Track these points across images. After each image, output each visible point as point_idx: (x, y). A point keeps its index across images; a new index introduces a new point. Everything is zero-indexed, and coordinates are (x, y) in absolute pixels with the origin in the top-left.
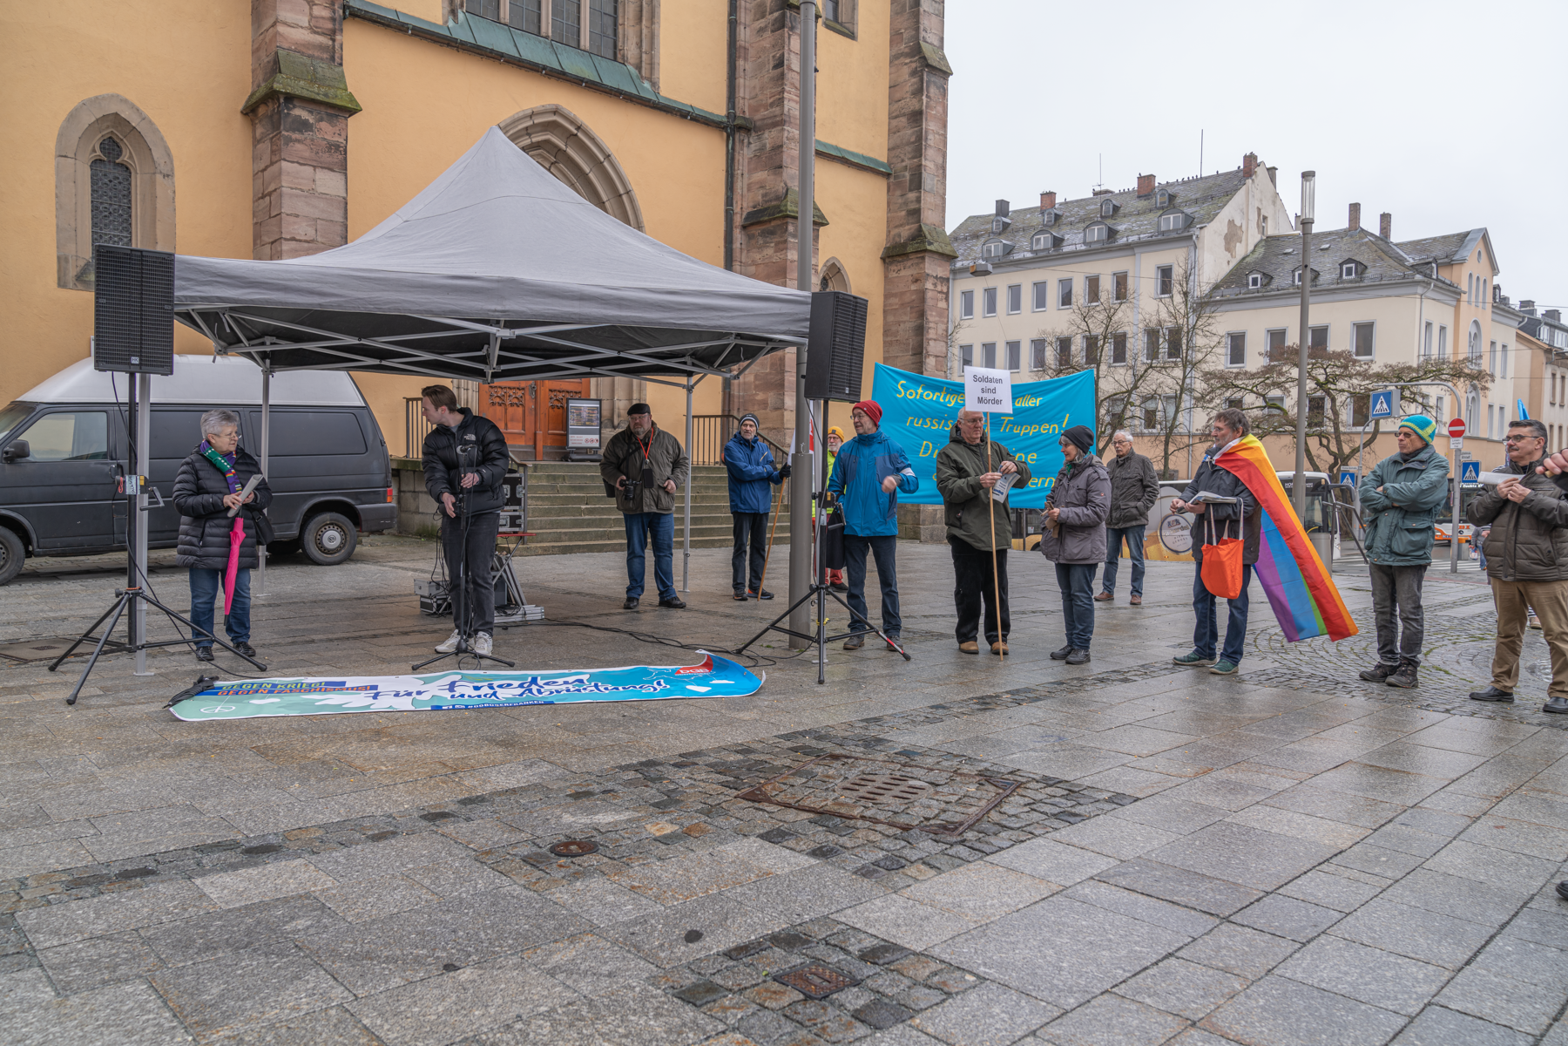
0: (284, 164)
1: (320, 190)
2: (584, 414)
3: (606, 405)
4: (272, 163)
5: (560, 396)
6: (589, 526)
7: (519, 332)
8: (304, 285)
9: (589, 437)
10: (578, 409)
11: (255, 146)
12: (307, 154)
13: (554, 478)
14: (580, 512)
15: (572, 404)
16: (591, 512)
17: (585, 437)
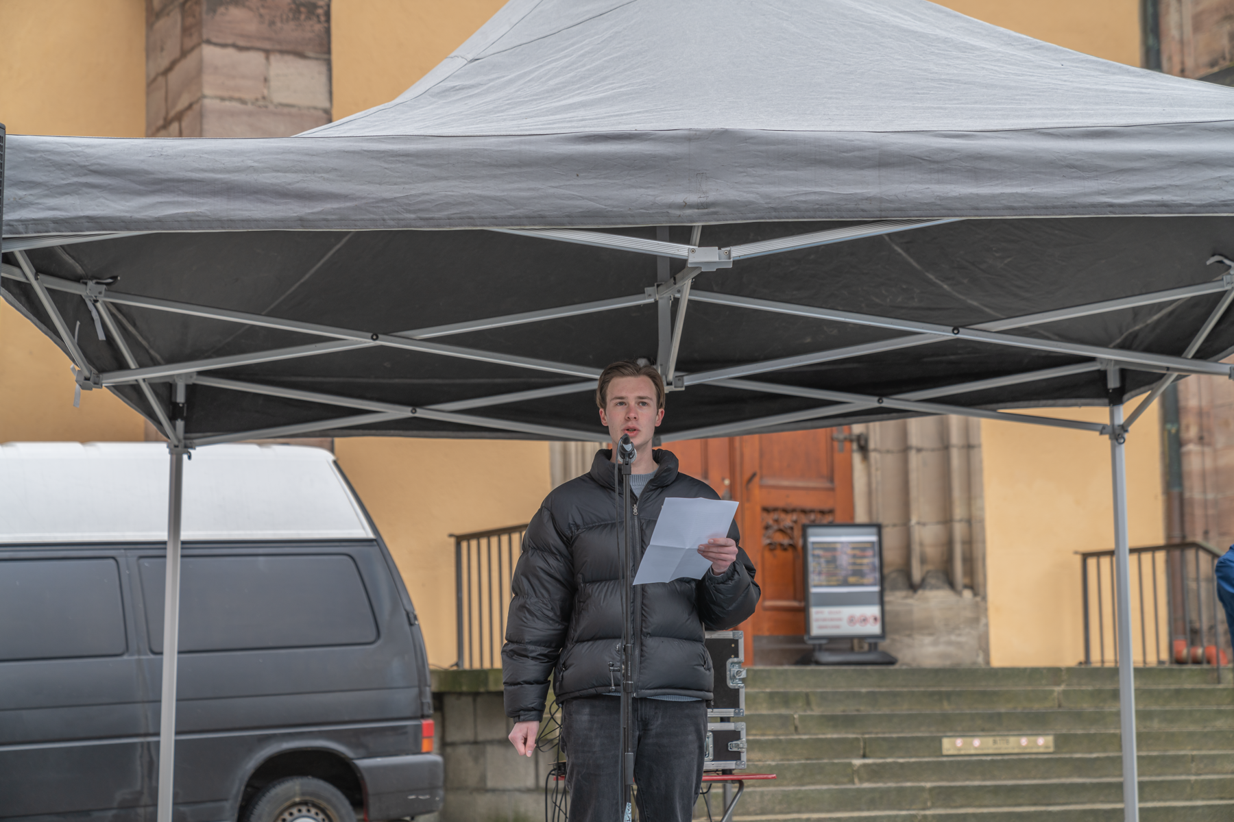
0: (208, 51)
1: (279, 97)
2: (844, 560)
3: (892, 538)
4: (184, 54)
5: (787, 520)
6: (872, 804)
7: (740, 251)
8: (268, 179)
10: (830, 548)
11: (150, 25)
12: (252, 27)
13: (787, 699)
14: (851, 773)
16: (875, 773)
17: (847, 611)
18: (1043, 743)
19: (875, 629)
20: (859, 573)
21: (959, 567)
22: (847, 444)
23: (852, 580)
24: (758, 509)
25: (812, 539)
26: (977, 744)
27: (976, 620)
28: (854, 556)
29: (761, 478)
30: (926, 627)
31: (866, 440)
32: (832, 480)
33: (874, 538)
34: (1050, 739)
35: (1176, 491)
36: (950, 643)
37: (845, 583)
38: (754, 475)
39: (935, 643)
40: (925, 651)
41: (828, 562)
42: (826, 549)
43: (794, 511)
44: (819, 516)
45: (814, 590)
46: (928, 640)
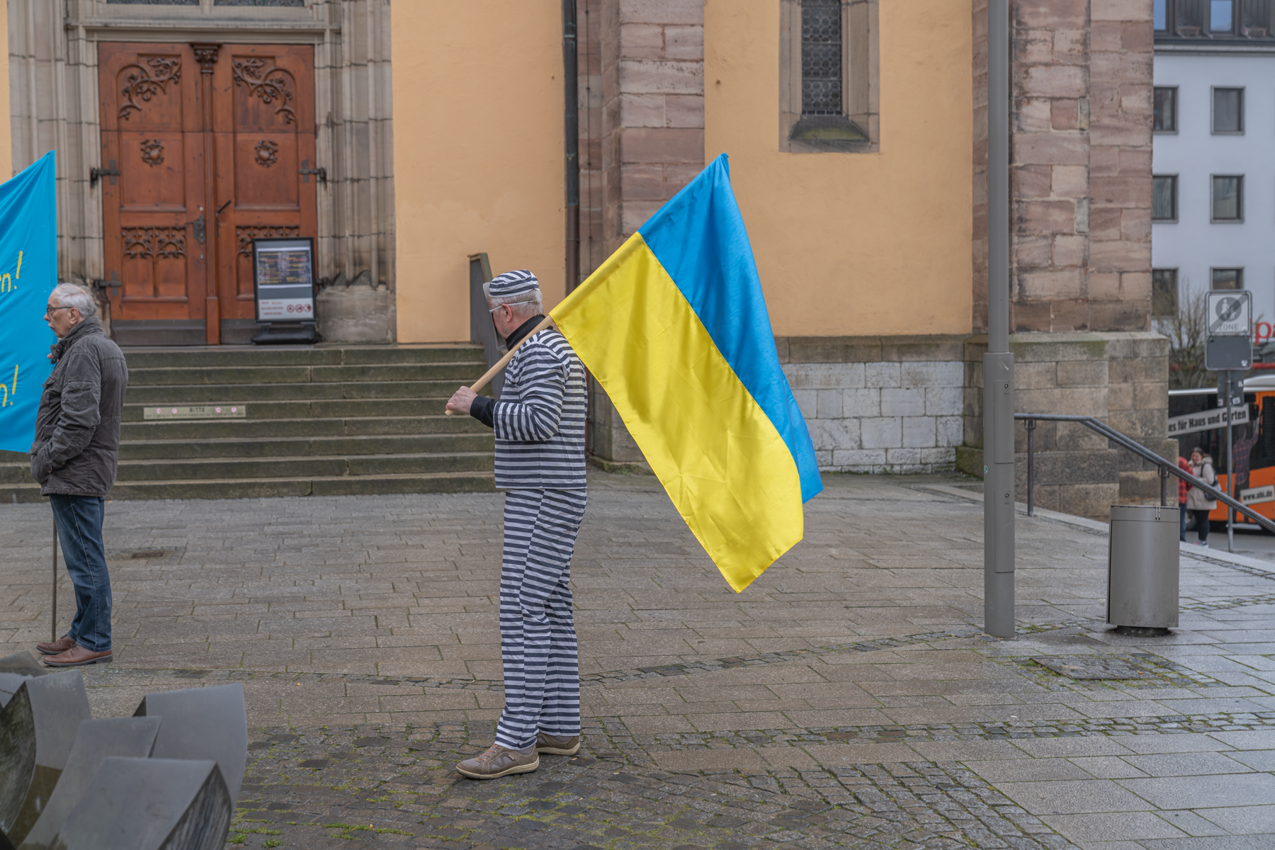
2: (283, 265)
3: (324, 245)
9: (295, 302)
10: (273, 256)
15: (261, 249)
18: (236, 411)
19: (309, 315)
20: (295, 274)
21: (377, 269)
22: (312, 177)
23: (289, 279)
24: (233, 227)
25: (259, 250)
26: (176, 412)
27: (386, 308)
28: (291, 262)
29: (236, 205)
30: (350, 313)
31: (325, 174)
32: (298, 204)
33: (308, 248)
34: (243, 408)
35: (573, 205)
36: (365, 325)
37: (284, 282)
38: (229, 203)
39: (356, 325)
40: (349, 331)
41: (271, 266)
42: (269, 257)
43: (264, 228)
44: (288, 231)
45: (260, 287)
46: (352, 322)
